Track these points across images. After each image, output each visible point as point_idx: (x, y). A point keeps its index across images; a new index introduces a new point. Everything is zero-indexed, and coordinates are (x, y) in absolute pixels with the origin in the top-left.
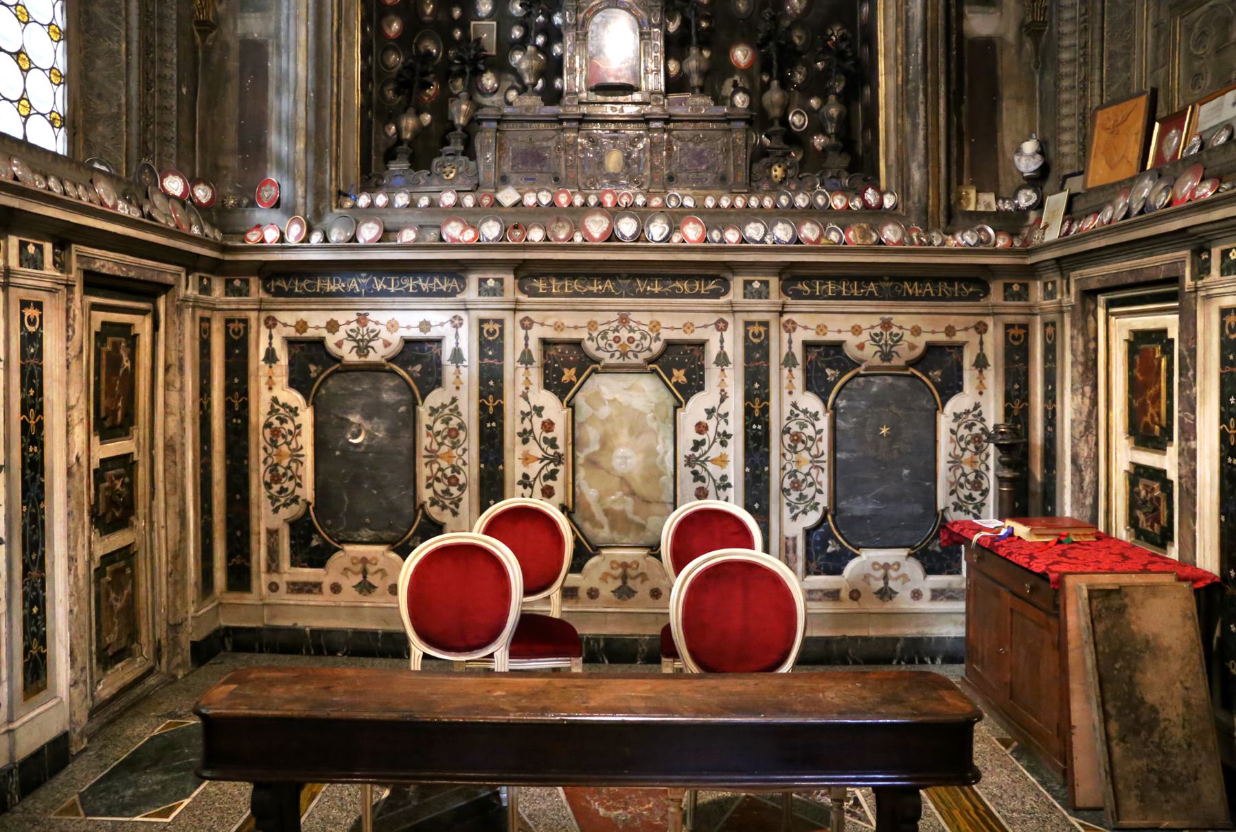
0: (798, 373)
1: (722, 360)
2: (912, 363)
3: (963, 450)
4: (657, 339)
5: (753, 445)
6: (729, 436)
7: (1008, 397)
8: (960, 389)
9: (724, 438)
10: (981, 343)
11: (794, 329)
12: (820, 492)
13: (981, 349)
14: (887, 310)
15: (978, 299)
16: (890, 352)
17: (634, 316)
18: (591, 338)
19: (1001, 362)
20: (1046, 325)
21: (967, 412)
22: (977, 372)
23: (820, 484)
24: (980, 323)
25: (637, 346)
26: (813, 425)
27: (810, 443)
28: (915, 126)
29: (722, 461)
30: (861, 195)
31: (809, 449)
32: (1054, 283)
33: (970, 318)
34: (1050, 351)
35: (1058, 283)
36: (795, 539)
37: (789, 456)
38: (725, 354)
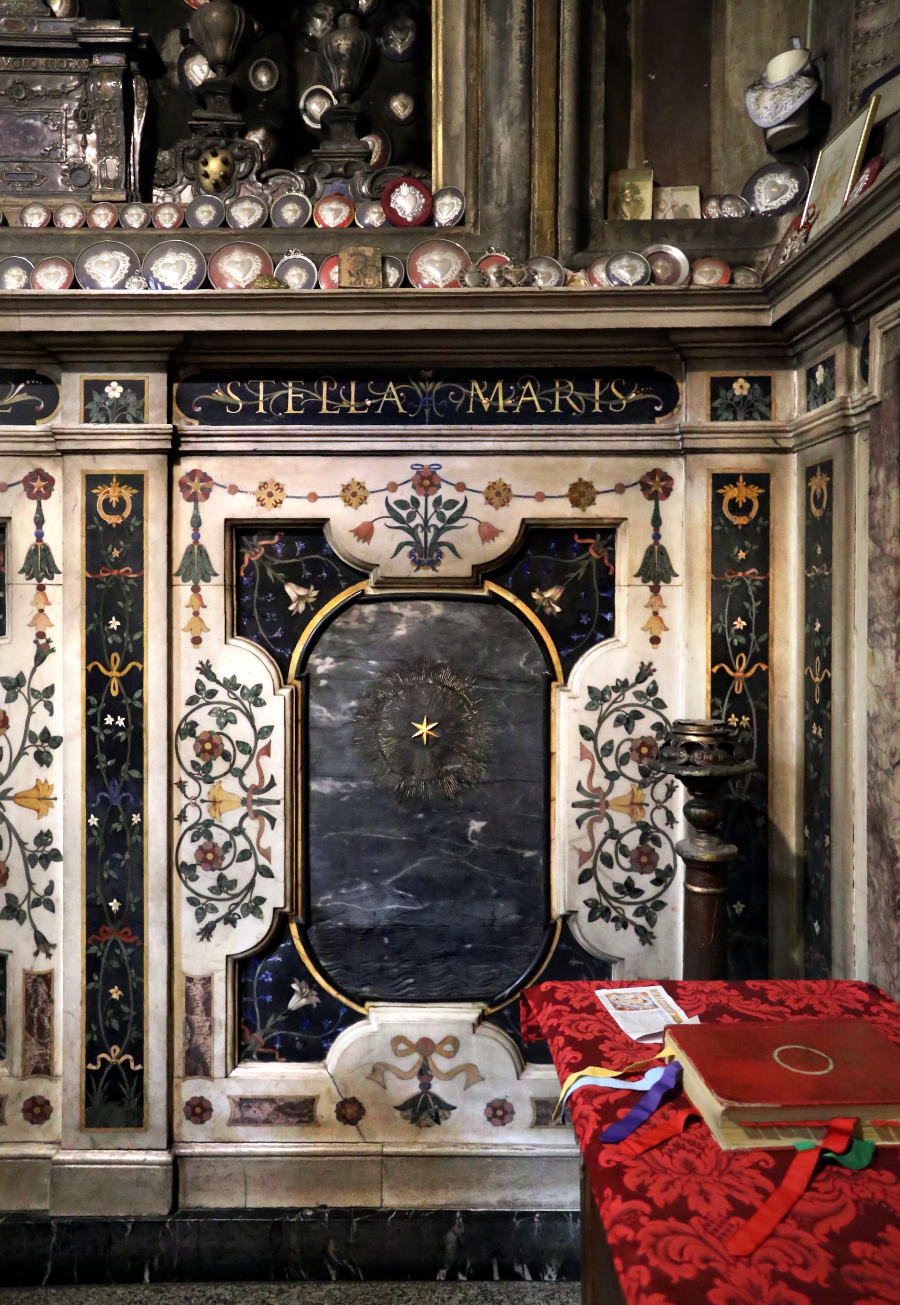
0: (214, 594)
1: (41, 564)
2: (484, 572)
3: (612, 776)
5: (105, 762)
6: (56, 742)
7: (720, 651)
8: (608, 630)
9: (45, 745)
10: (657, 521)
11: (206, 493)
12: (267, 873)
13: (657, 536)
14: (427, 446)
15: (651, 418)
16: (436, 544)
19: (703, 563)
20: (809, 473)
21: (622, 686)
22: (645, 591)
23: (267, 854)
24: (653, 473)
26: (251, 718)
27: (241, 760)
28: (503, 35)
29: (39, 798)
30: (382, 196)
31: (240, 774)
32: (829, 364)
33: (631, 461)
34: (818, 532)
35: (840, 362)
36: (207, 981)
37: (192, 788)
38: (46, 550)
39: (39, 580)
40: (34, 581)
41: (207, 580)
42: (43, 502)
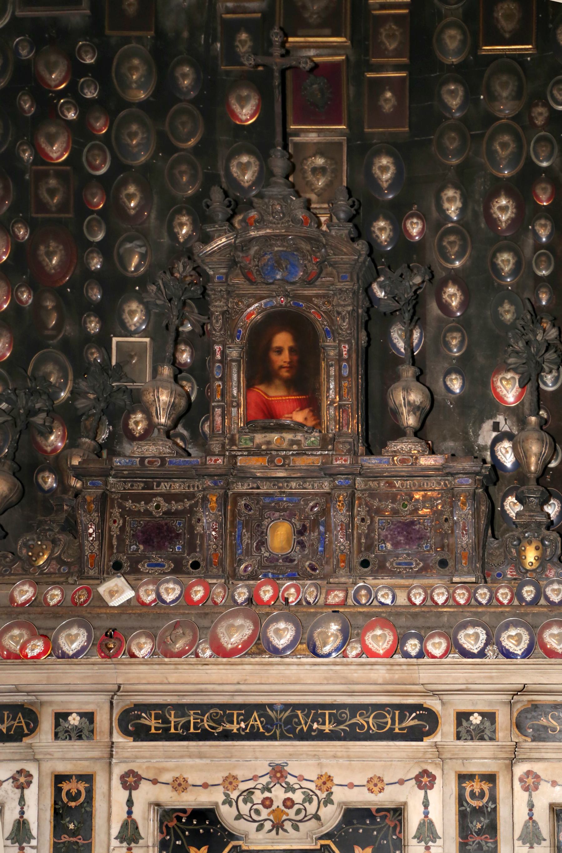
1: (427, 832)
4: (328, 801)
17: (293, 768)
18: (228, 801)
25: (298, 812)
38: (431, 823)
39: (426, 843)
40: (423, 843)
41: (539, 843)
42: (428, 791)
